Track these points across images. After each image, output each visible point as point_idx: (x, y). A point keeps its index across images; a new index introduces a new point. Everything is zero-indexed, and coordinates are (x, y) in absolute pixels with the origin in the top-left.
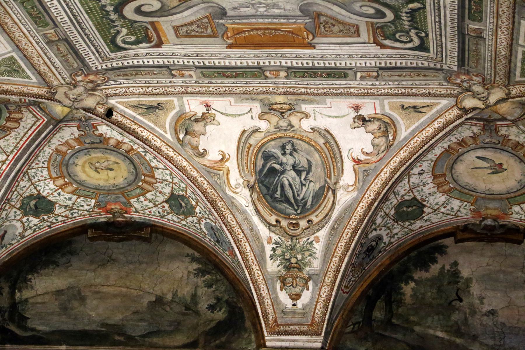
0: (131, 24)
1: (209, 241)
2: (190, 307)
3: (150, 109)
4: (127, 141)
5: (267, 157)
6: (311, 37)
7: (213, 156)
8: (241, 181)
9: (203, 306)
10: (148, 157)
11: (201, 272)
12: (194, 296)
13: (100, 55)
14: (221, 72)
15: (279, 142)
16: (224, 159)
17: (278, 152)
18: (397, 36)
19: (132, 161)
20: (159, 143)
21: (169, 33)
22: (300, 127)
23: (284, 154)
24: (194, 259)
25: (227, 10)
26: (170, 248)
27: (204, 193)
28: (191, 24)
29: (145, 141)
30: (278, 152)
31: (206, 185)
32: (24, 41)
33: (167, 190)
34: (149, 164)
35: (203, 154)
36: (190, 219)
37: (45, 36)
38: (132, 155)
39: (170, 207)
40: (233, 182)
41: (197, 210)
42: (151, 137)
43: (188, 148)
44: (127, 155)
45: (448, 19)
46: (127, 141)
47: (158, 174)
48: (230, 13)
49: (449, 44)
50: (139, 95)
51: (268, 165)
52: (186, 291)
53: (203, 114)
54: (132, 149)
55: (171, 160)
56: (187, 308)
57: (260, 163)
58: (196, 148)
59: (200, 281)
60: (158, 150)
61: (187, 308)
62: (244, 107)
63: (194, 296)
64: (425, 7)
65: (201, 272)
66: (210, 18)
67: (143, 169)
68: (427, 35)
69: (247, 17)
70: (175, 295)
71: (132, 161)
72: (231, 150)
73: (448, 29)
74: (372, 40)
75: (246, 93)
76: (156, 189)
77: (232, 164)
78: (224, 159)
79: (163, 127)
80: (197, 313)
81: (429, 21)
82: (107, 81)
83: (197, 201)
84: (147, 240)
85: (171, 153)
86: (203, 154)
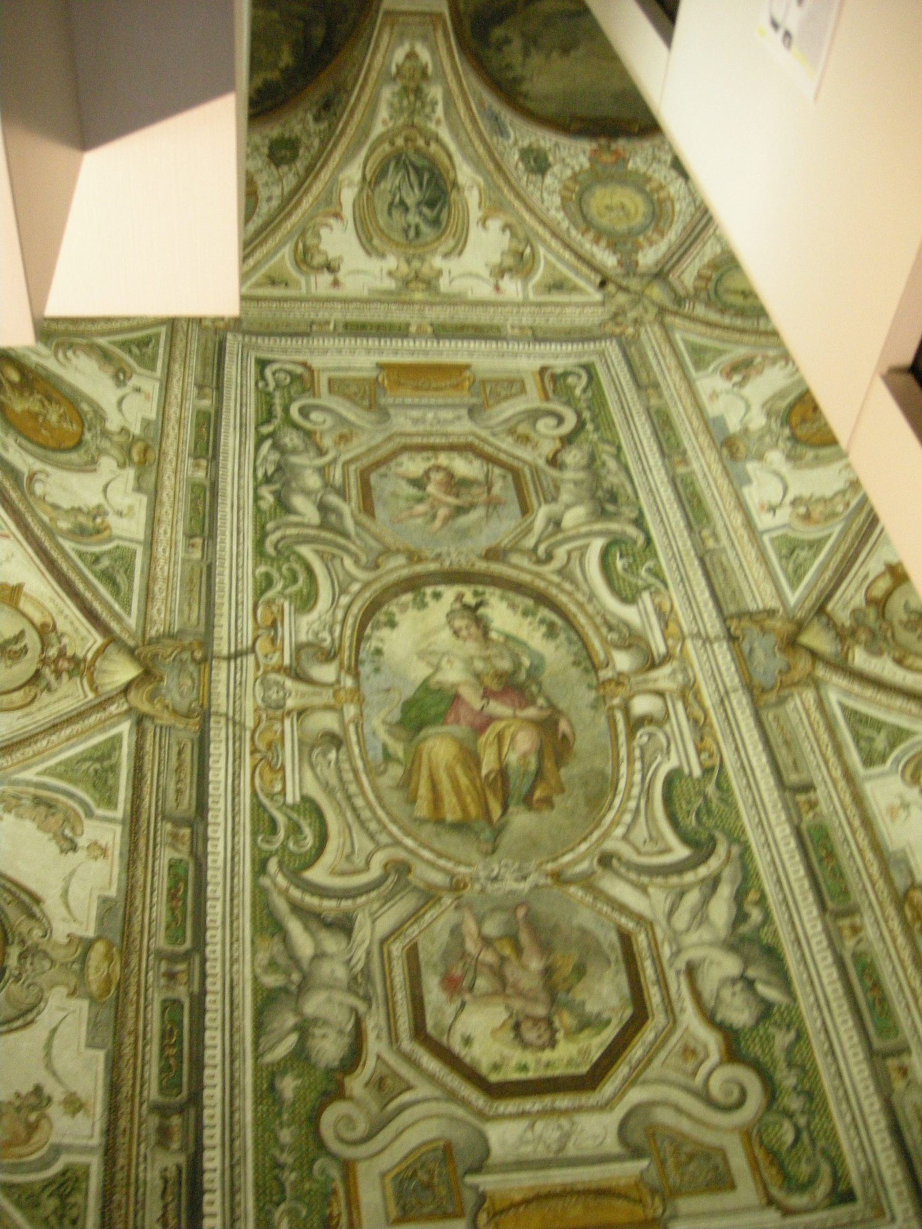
0: (570, 401)
1: (507, 116)
2: (531, 42)
3: (558, 285)
4: (587, 245)
5: (435, 223)
6: (380, 379)
7: (495, 225)
8: (466, 193)
9: (517, 44)
10: (565, 224)
11: (518, 81)
12: (526, 53)
13: (606, 362)
14: (480, 333)
15: (421, 240)
16: (483, 222)
17: (424, 228)
18: (288, 380)
19: (584, 217)
20: (554, 243)
21: (532, 386)
22: (398, 260)
23: (417, 228)
24: (526, 96)
25: (466, 416)
26: (551, 109)
27: (507, 180)
28: (507, 398)
29: (567, 246)
30: (424, 228)
31: (506, 190)
32: (683, 391)
33: (549, 180)
34: (566, 214)
35: (507, 227)
36: (526, 144)
37: (660, 396)
38: (583, 226)
39: (546, 159)
40: (475, 193)
41: (517, 157)
42: (561, 251)
43: (521, 234)
44: (587, 224)
45: (232, 411)
46: (587, 245)
47: (557, 200)
48: (464, 412)
49: (234, 373)
50: (569, 304)
51: (436, 211)
52: (536, 59)
53: (502, 277)
54: (583, 235)
55: (542, 222)
56: (535, 42)
57: (444, 215)
58: (514, 235)
59: (519, 71)
60: (555, 235)
61: (535, 42)
62: (459, 285)
63: (526, 53)
64: (256, 428)
65: (518, 81)
66: (485, 406)
67: (573, 208)
68: (256, 384)
69: (445, 406)
70: (548, 56)
71: (584, 217)
72: (475, 232)
73: (233, 397)
74: (316, 374)
75: (454, 304)
76: (560, 181)
77: (475, 213)
78: (483, 222)
79: (547, 262)
80: (523, 35)
81: (253, 406)
82: (602, 324)
83: (516, 167)
84: (574, 118)
85: (540, 230)
86: (507, 227)
